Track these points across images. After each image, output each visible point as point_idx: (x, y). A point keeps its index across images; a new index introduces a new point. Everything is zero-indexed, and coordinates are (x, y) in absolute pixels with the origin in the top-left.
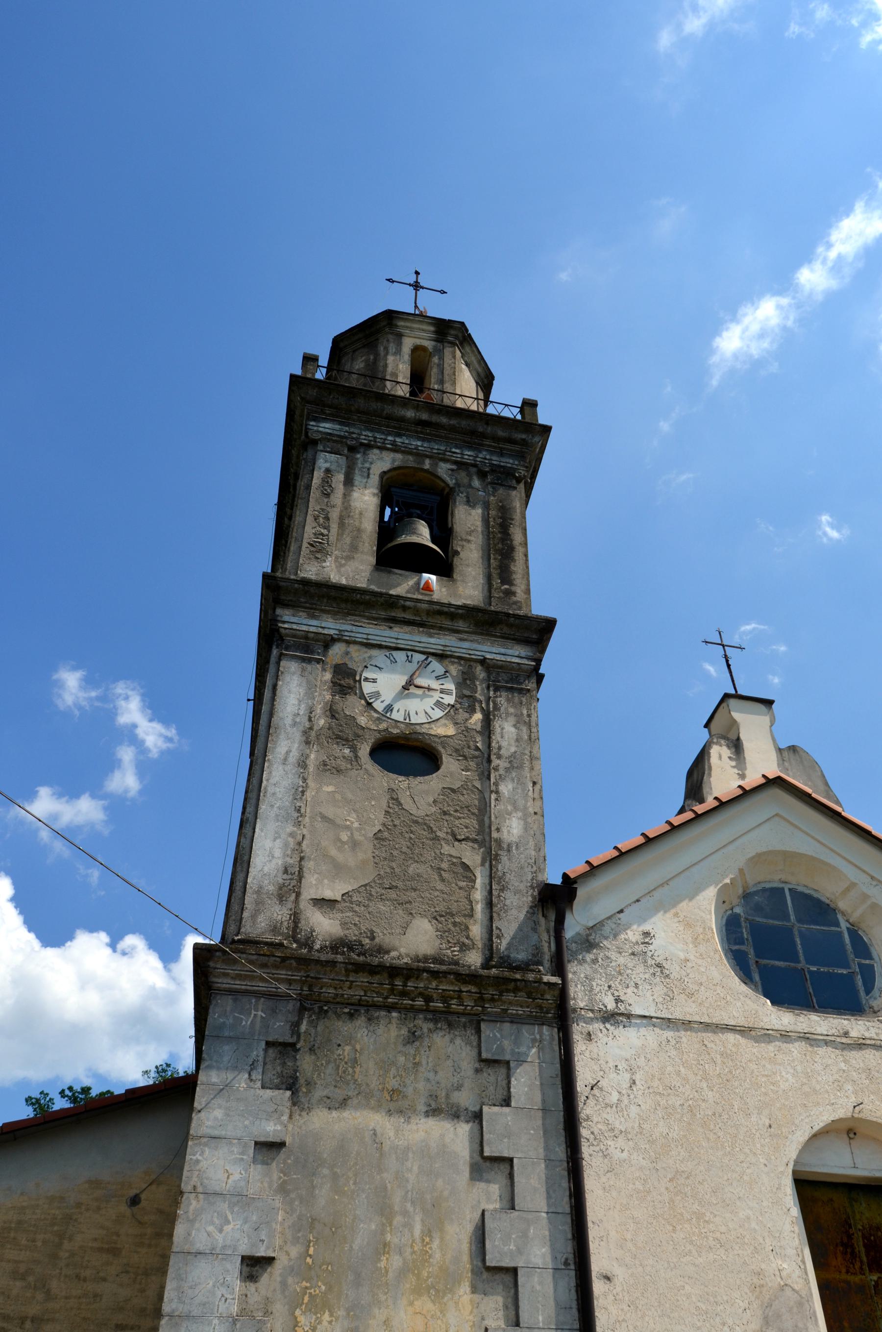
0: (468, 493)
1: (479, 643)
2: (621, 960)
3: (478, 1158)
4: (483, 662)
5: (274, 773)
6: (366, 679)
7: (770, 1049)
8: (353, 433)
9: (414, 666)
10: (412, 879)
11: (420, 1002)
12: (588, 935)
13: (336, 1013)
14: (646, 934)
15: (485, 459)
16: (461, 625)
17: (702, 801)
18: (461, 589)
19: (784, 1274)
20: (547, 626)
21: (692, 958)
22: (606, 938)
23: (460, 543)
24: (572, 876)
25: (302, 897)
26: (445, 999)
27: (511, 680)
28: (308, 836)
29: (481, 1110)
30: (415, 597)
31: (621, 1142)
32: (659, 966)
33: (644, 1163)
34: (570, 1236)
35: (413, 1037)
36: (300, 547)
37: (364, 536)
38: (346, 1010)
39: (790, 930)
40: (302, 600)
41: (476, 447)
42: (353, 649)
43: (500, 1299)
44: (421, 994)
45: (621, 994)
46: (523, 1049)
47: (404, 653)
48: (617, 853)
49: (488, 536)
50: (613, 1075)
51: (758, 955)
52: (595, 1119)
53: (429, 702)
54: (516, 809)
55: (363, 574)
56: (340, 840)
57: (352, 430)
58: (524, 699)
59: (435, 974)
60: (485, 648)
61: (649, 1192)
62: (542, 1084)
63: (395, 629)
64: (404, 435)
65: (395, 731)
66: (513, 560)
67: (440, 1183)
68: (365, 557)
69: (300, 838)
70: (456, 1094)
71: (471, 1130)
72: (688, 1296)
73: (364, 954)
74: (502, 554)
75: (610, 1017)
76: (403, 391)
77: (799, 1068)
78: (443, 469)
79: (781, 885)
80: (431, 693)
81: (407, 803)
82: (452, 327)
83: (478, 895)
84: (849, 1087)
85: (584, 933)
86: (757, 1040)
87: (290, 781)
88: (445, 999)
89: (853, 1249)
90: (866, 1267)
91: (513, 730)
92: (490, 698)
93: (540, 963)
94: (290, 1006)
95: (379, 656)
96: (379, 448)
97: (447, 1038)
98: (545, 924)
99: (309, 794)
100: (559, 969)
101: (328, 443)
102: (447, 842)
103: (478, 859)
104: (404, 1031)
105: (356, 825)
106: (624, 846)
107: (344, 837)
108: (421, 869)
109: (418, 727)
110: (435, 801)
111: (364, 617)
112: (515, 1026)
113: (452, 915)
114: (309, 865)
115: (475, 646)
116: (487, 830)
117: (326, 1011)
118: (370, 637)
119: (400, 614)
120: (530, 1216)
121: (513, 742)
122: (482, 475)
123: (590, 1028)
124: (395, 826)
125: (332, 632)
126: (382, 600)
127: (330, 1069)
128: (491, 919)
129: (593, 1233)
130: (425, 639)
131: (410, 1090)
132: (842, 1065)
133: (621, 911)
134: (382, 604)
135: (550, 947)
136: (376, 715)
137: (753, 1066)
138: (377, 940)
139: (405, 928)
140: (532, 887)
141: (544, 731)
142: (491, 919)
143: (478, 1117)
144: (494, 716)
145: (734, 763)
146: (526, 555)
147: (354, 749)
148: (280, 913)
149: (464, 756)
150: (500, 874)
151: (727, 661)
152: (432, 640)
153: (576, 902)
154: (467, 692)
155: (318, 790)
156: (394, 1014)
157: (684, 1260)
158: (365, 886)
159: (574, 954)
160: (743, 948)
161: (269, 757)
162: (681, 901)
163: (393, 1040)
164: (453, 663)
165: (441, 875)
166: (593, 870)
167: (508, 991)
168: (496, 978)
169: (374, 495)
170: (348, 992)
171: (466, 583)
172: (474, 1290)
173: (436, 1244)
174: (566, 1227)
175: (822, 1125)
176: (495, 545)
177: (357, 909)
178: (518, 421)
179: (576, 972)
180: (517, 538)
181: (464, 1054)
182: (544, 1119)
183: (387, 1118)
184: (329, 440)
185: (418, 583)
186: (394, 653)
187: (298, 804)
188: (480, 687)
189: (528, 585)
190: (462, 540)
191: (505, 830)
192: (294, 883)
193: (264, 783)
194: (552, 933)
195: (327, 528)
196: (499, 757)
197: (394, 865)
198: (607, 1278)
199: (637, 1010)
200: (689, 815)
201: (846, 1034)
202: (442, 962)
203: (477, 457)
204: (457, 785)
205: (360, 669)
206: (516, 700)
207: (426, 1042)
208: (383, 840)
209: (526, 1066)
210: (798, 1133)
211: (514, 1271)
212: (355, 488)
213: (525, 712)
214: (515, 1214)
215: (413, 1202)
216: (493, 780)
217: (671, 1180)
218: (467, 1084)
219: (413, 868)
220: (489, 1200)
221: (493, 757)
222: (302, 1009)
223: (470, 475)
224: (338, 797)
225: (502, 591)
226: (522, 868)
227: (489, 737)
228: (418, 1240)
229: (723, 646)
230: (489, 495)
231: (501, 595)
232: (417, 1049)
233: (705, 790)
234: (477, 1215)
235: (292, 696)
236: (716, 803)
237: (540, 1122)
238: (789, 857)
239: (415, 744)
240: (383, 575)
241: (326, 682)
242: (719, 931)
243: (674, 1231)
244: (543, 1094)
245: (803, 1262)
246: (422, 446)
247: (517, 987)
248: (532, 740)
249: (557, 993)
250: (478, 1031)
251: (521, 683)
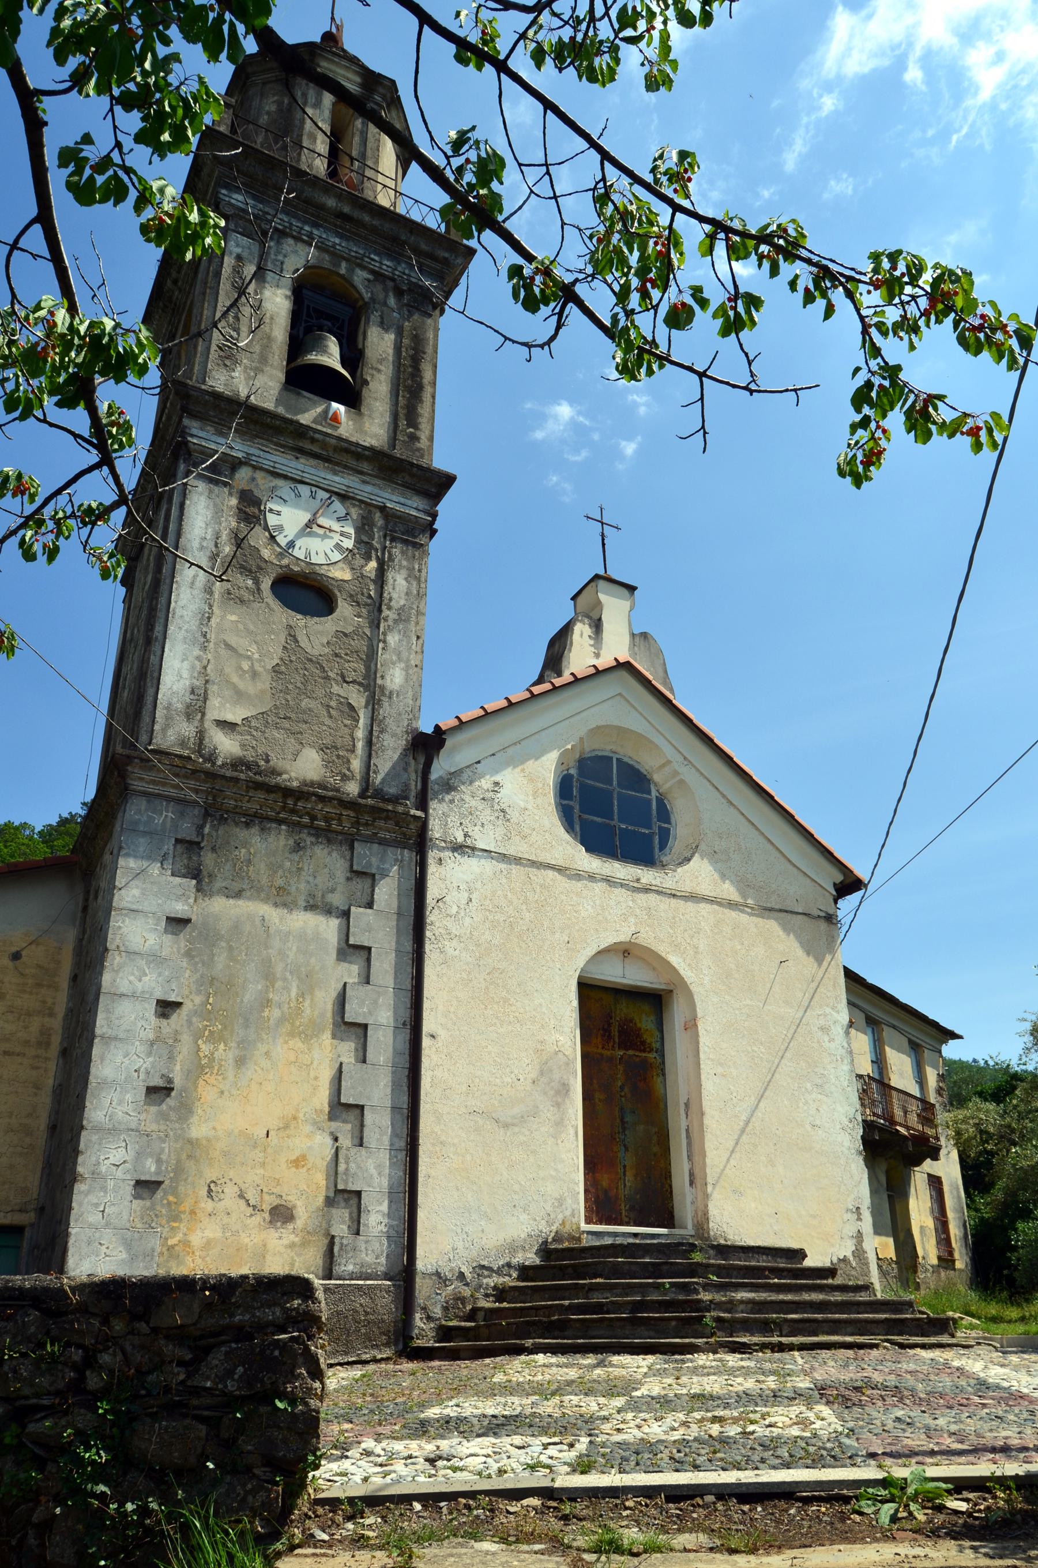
0: (382, 312)
1: (380, 488)
2: (473, 803)
3: (344, 945)
4: (383, 509)
5: (182, 596)
6: (271, 511)
7: (579, 885)
8: (268, 213)
9: (317, 503)
10: (304, 712)
11: (306, 820)
12: (449, 779)
13: (234, 821)
14: (497, 784)
15: (404, 273)
16: (365, 466)
17: (559, 674)
18: (367, 425)
20: (447, 481)
21: (530, 807)
22: (463, 783)
23: (370, 371)
24: (444, 728)
25: (207, 717)
26: (327, 819)
27: (407, 532)
28: (212, 661)
29: (349, 910)
30: (324, 430)
31: (455, 943)
32: (503, 811)
33: (470, 960)
34: (409, 1006)
35: (298, 848)
36: (208, 349)
37: (274, 347)
38: (243, 820)
39: (610, 793)
40: (211, 413)
41: (396, 256)
42: (259, 475)
43: (353, 1045)
44: (308, 814)
45: (470, 830)
46: (387, 866)
47: (309, 487)
48: (482, 713)
49: (399, 368)
50: (455, 893)
51: (581, 811)
52: (437, 924)
53: (330, 543)
54: (400, 659)
55: (272, 392)
56: (241, 668)
57: (267, 209)
58: (417, 554)
59: (322, 799)
60: (386, 495)
61: (471, 981)
62: (399, 894)
63: (302, 460)
64: (321, 226)
65: (296, 569)
66: (421, 401)
67: (313, 960)
68: (274, 372)
69: (205, 662)
70: (330, 895)
71: (340, 924)
72: (490, 1053)
73: (260, 774)
74: (410, 392)
75: (458, 848)
76: (320, 166)
78: (360, 277)
79: (611, 755)
80: (332, 534)
81: (304, 642)
82: (381, 84)
83: (360, 734)
85: (446, 777)
86: (570, 877)
87: (197, 606)
88: (327, 819)
91: (404, 583)
92: (385, 547)
93: (407, 798)
94: (196, 811)
95: (285, 488)
96: (293, 237)
97: (326, 851)
98: (415, 767)
99: (214, 621)
100: (423, 805)
101: (240, 222)
102: (337, 684)
103: (363, 701)
104: (291, 842)
105: (256, 656)
106: (490, 707)
107: (246, 665)
108: (312, 704)
109: (317, 568)
110: (328, 643)
111: (271, 442)
112: (382, 847)
113: (337, 749)
114: (213, 689)
115: (376, 491)
116: (373, 676)
117: (226, 819)
118: (277, 465)
119: (308, 446)
120: (381, 990)
121: (403, 595)
122: (399, 293)
123: (442, 855)
124: (291, 661)
125: (240, 455)
126: (291, 428)
127: (228, 866)
128: (370, 756)
129: (426, 1005)
130: (329, 476)
131: (293, 889)
133: (479, 762)
134: (291, 432)
135: (416, 785)
136: (279, 550)
138: (271, 763)
139: (296, 755)
140: (407, 732)
141: (432, 588)
142: (370, 756)
143: (346, 914)
144: (388, 566)
145: (592, 642)
146: (434, 397)
147: (257, 582)
148: (187, 729)
149: (357, 602)
150: (381, 717)
151: (603, 540)
152: (337, 479)
153: (442, 751)
154: (365, 538)
155: (223, 618)
156: (283, 827)
157: (490, 1029)
158: (263, 713)
159: (436, 795)
160: (571, 803)
161: (177, 578)
162: (529, 759)
163: (281, 848)
164: (354, 506)
165: (329, 712)
166: (462, 725)
167: (380, 818)
168: (372, 807)
169: (287, 297)
170: (246, 805)
171: (373, 419)
172: (334, 1036)
173: (307, 1003)
174: (407, 999)
176: (405, 380)
177: (255, 733)
178: (440, 234)
179: (437, 808)
180: (427, 375)
181: (338, 865)
182: (398, 920)
183: (273, 909)
184: (241, 218)
185: (326, 411)
186: (299, 486)
187: (204, 630)
188: (377, 534)
189: (432, 431)
190: (372, 368)
191: (388, 678)
192: (200, 703)
193: (173, 605)
194: (420, 774)
195: (237, 330)
196: (389, 608)
197: (288, 697)
198: (433, 1036)
199: (481, 845)
200: (546, 686)
202: (325, 788)
203: (396, 269)
204: (349, 629)
205: (265, 499)
206: (410, 553)
207: (309, 852)
208: (280, 673)
209: (387, 880)
211: (365, 1027)
212: (267, 285)
213: (417, 567)
214: (369, 987)
215: (291, 972)
216: (382, 629)
217: (489, 974)
218: (340, 888)
219: (305, 703)
220: (350, 975)
221: (384, 607)
222: (207, 814)
223: (386, 290)
224: (241, 627)
225: (407, 434)
226: (400, 714)
227: (382, 587)
228: (294, 999)
229: (602, 523)
230: (404, 319)
231: (406, 438)
232: (301, 857)
233: (564, 663)
234: (340, 986)
235: (200, 518)
236: (572, 679)
237: (395, 923)
238: (622, 732)
239: (312, 583)
240: (293, 396)
241: (231, 507)
242: (555, 787)
243: (486, 1009)
244: (399, 902)
246: (340, 245)
247: (388, 815)
248: (420, 595)
249: (420, 824)
250: (352, 848)
251: (416, 537)
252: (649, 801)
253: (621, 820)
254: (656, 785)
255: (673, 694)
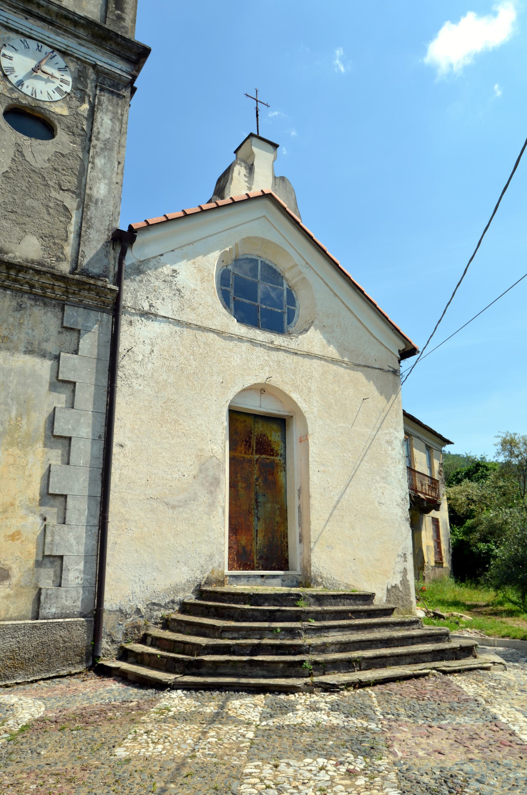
1: (93, 51)
2: (157, 284)
3: (55, 380)
4: (94, 66)
9: (42, 55)
10: (28, 209)
11: (26, 288)
12: (139, 266)
14: (175, 271)
16: (81, 32)
17: (222, 198)
19: (214, 451)
21: (198, 289)
22: (150, 269)
27: (113, 86)
29: (59, 355)
31: (140, 381)
32: (179, 290)
33: (151, 393)
34: (104, 424)
43: (60, 452)
44: (27, 283)
45: (154, 302)
46: (89, 324)
47: (36, 42)
48: (165, 219)
50: (141, 346)
52: (127, 367)
53: (51, 87)
54: (104, 177)
58: (120, 102)
62: (98, 345)
65: (24, 102)
67: (30, 391)
71: (52, 365)
72: (163, 457)
75: (145, 314)
77: (244, 356)
80: (54, 80)
81: (29, 157)
83: (72, 228)
84: (267, 369)
85: (137, 264)
86: (225, 338)
88: (43, 288)
89: (250, 443)
90: (254, 452)
91: (109, 122)
92: (96, 95)
93: (106, 277)
95: (16, 40)
97: (42, 311)
100: (118, 282)
102: (55, 190)
103: (75, 205)
104: (14, 303)
106: (170, 216)
108: (35, 204)
109: (41, 103)
110: (48, 160)
112: (86, 311)
113: (53, 238)
115: (90, 52)
116: (83, 187)
118: (9, 21)
120: (82, 413)
121: (108, 131)
124: (18, 170)
130: (52, 36)
131: (15, 338)
132: (266, 358)
133: (162, 255)
135: (114, 268)
136: (10, 86)
137: (220, 352)
139: (20, 240)
142: (79, 244)
143: (57, 358)
144: (98, 109)
149: (73, 132)
150: (88, 217)
153: (135, 244)
154: (81, 87)
156: (8, 292)
157: (164, 441)
159: (129, 276)
162: (199, 256)
164: (72, 61)
165: (48, 211)
166: (149, 226)
167: (84, 289)
168: (78, 281)
172: (45, 446)
173: (24, 422)
174: (102, 420)
175: (249, 385)
181: (52, 322)
182: (97, 363)
186: (29, 41)
189: (135, 16)
191: (95, 190)
194: (117, 260)
196: (98, 139)
197: (16, 197)
198: (122, 446)
199: (161, 313)
200: (213, 205)
201: (272, 342)
202: (43, 265)
204: (66, 152)
207: (28, 312)
208: (9, 178)
210: (236, 387)
211: (70, 439)
213: (120, 112)
214: (73, 411)
215: (12, 399)
216: (91, 154)
217: (164, 403)
218: (52, 339)
219: (29, 202)
220: (59, 402)
221: (93, 138)
225: (115, 14)
227: (92, 124)
228: (13, 419)
231: (114, 18)
232: (22, 315)
233: (226, 192)
236: (231, 201)
237: (95, 365)
238: (265, 242)
239: (38, 115)
243: (162, 426)
244: (99, 350)
245: (225, 447)
247: (90, 288)
250: (63, 310)
251: (120, 90)
252: (283, 290)
253: (261, 303)
254: (287, 280)
255: (301, 219)
